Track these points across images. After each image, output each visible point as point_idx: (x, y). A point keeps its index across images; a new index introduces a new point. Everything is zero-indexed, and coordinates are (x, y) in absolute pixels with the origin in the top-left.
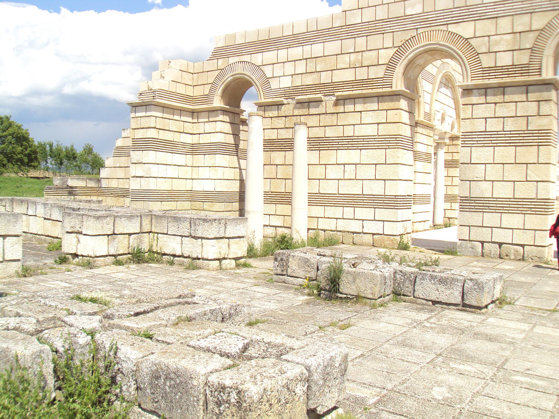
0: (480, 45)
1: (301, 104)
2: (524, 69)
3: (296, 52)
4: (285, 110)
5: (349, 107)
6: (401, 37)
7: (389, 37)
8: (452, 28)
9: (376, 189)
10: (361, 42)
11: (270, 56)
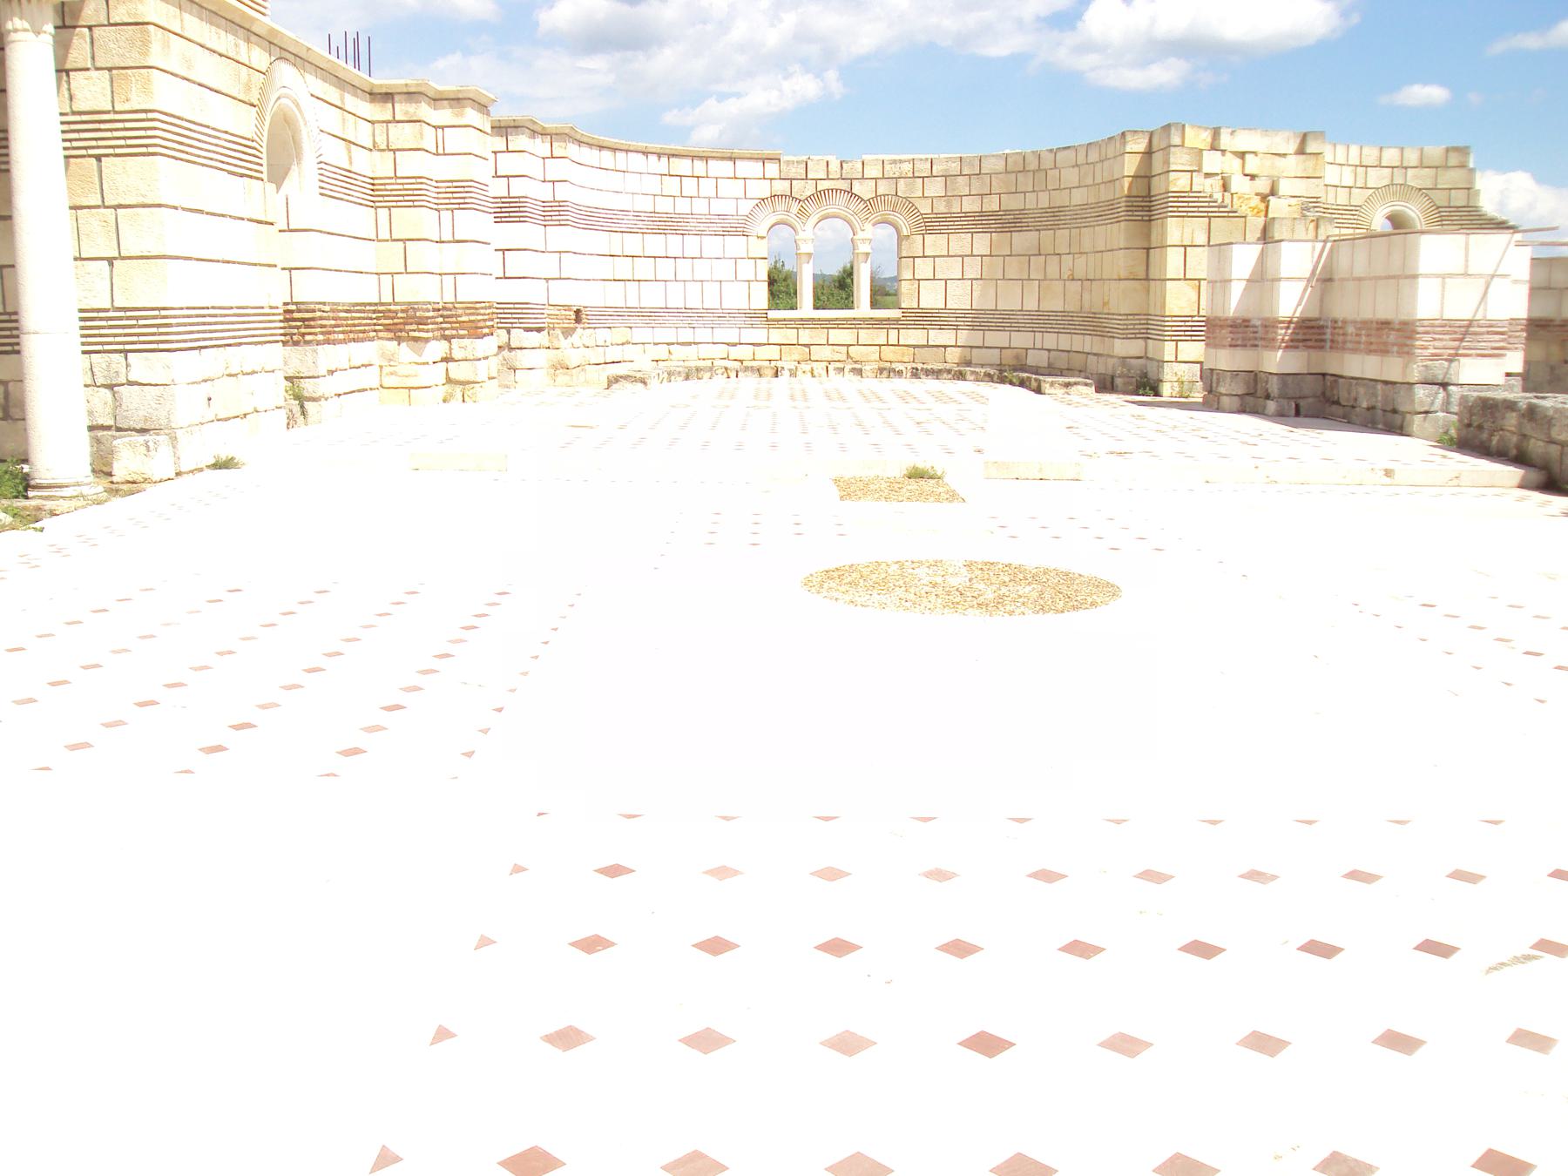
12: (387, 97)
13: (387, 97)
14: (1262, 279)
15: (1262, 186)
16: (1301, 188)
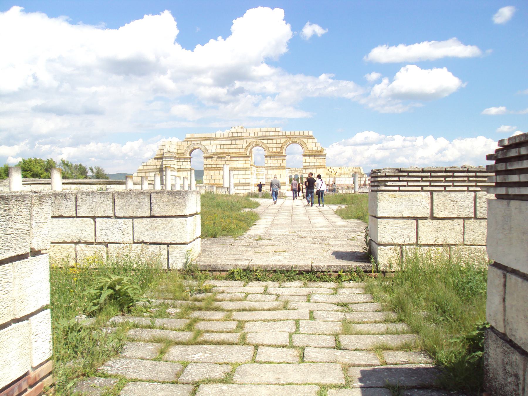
0: (269, 145)
2: (279, 152)
3: (217, 142)
4: (213, 159)
5: (235, 159)
6: (249, 142)
7: (245, 141)
8: (262, 141)
9: (243, 181)
10: (237, 142)
11: (208, 143)
12: (258, 167)
13: (258, 167)
14: (330, 181)
15: (336, 172)
16: (339, 172)
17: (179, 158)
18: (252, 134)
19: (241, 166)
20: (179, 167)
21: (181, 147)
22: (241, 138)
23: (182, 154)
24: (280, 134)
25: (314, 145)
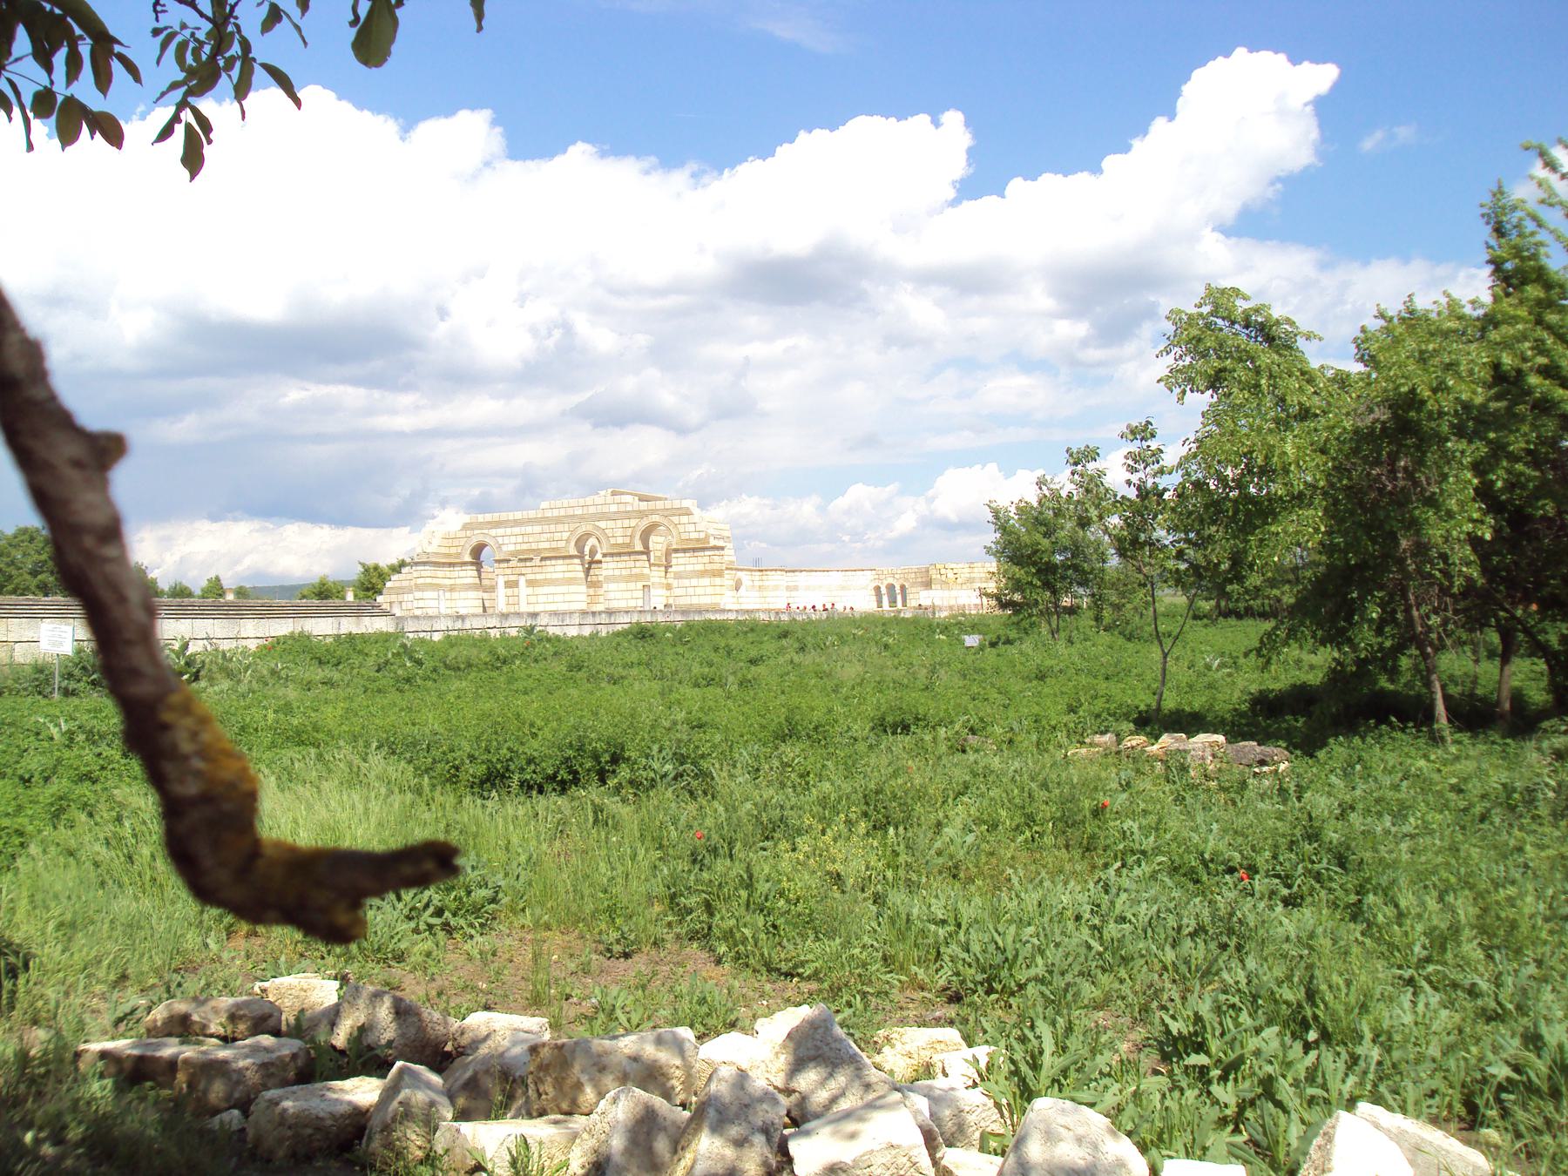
1: (520, 560)
2: (628, 545)
3: (516, 530)
5: (548, 562)
6: (573, 526)
11: (500, 531)
17: (451, 565)
18: (579, 512)
19: (560, 576)
20: (452, 582)
21: (456, 542)
22: (558, 520)
23: (459, 555)
24: (629, 508)
25: (691, 528)
